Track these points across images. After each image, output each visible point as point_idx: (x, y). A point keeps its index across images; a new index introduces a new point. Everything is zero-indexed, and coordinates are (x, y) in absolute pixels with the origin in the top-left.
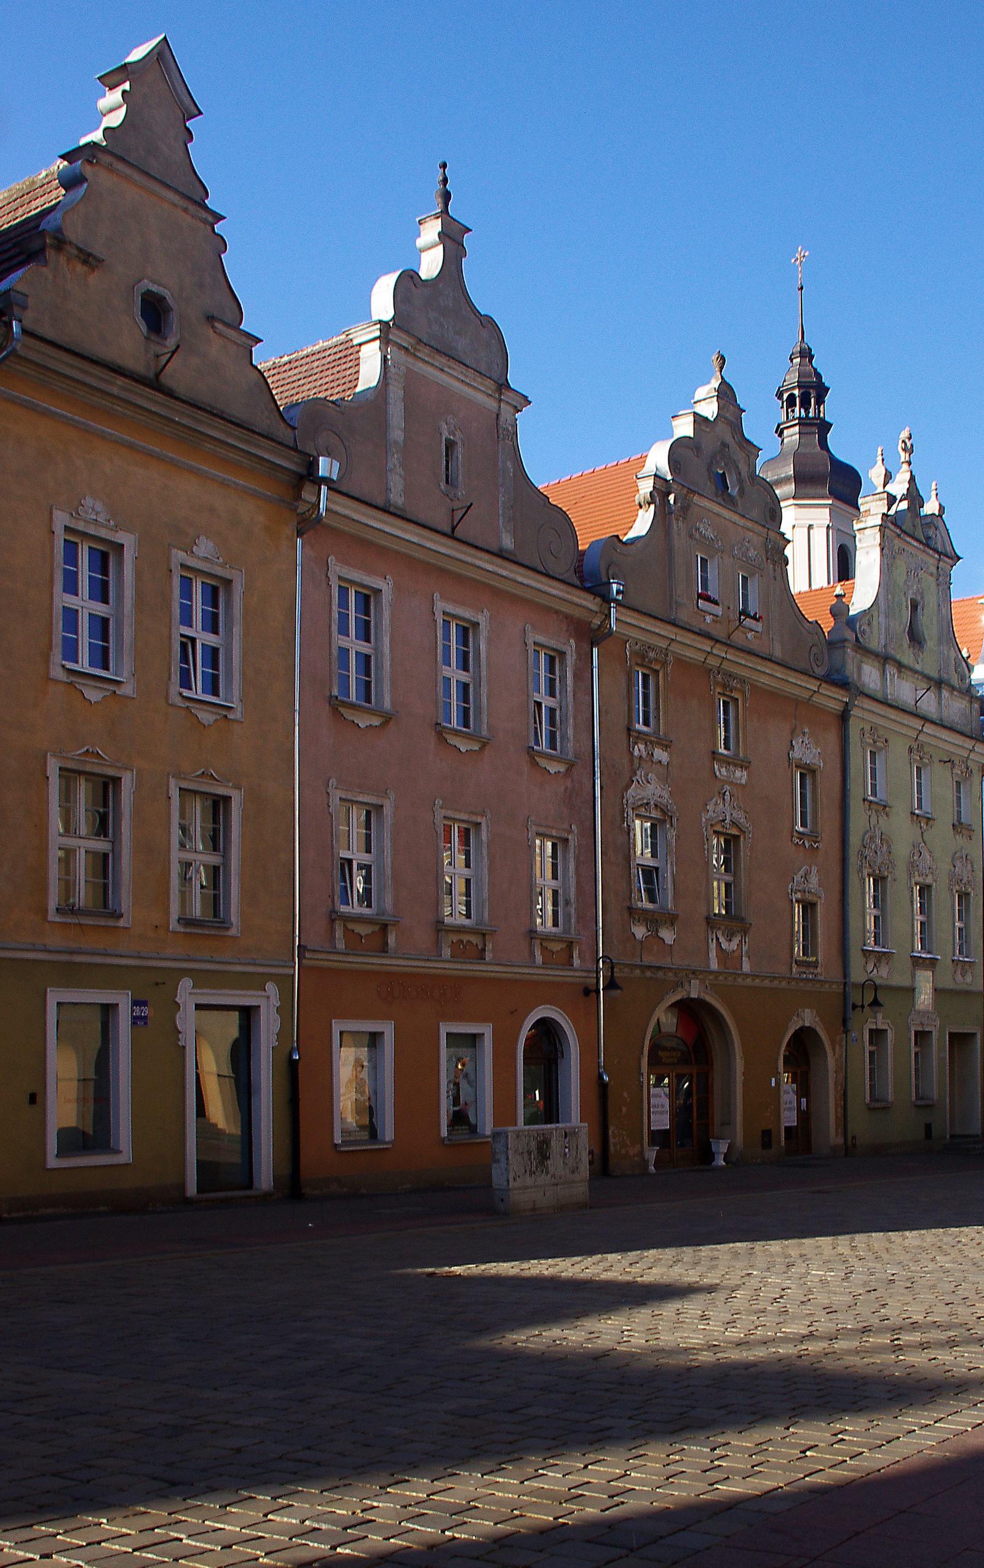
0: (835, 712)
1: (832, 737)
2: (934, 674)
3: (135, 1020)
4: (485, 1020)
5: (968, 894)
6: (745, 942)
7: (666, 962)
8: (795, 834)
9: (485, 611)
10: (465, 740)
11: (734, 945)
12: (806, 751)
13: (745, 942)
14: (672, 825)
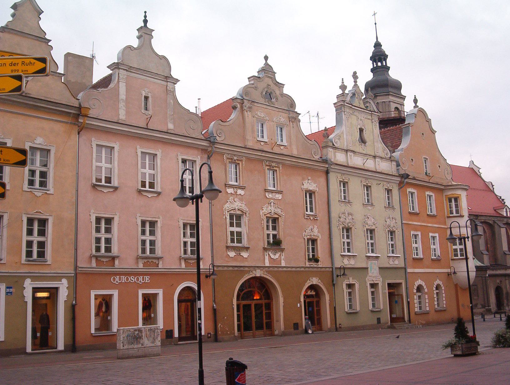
0: (325, 171)
1: (322, 180)
2: (373, 154)
3: (7, 293)
5: (395, 231)
6: (282, 255)
7: (246, 264)
8: (305, 215)
9: (159, 150)
10: (150, 194)
11: (277, 256)
12: (310, 185)
13: (282, 255)
14: (246, 216)
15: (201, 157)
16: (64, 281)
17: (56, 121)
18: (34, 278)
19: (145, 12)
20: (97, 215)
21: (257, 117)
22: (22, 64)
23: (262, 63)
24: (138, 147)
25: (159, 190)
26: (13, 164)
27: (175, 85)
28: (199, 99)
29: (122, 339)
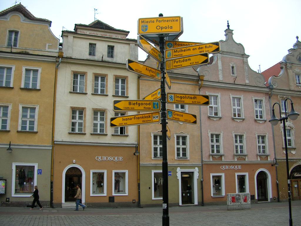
4: (246, 172)
14: (293, 130)
15: (265, 98)
16: (197, 169)
17: (188, 84)
18: (182, 167)
19: (228, 21)
20: (212, 133)
21: (295, 72)
22: (205, 47)
23: (295, 41)
24: (231, 94)
25: (243, 118)
26: (202, 104)
27: (248, 59)
28: (260, 65)
29: (230, 200)
